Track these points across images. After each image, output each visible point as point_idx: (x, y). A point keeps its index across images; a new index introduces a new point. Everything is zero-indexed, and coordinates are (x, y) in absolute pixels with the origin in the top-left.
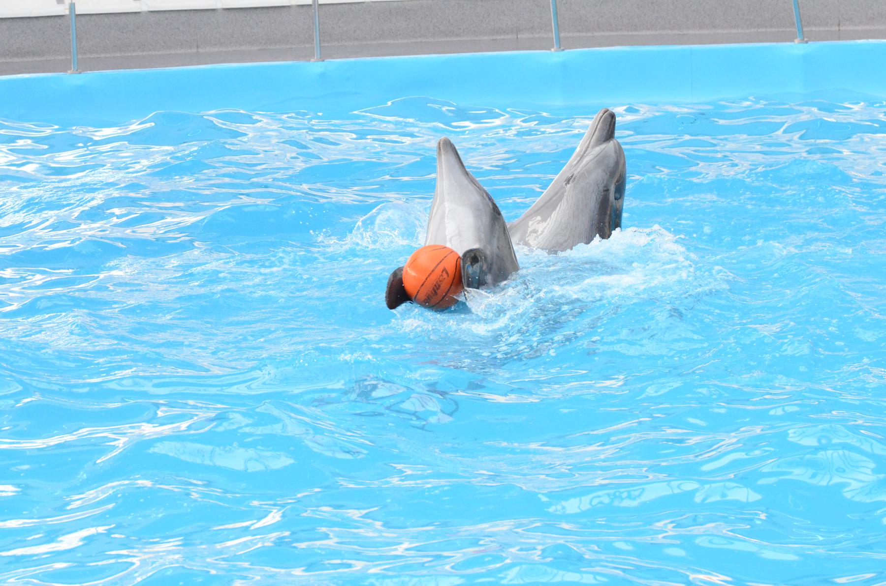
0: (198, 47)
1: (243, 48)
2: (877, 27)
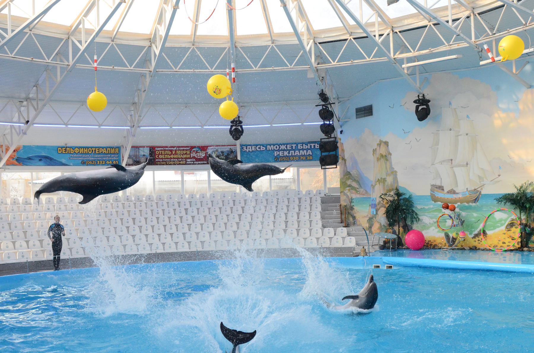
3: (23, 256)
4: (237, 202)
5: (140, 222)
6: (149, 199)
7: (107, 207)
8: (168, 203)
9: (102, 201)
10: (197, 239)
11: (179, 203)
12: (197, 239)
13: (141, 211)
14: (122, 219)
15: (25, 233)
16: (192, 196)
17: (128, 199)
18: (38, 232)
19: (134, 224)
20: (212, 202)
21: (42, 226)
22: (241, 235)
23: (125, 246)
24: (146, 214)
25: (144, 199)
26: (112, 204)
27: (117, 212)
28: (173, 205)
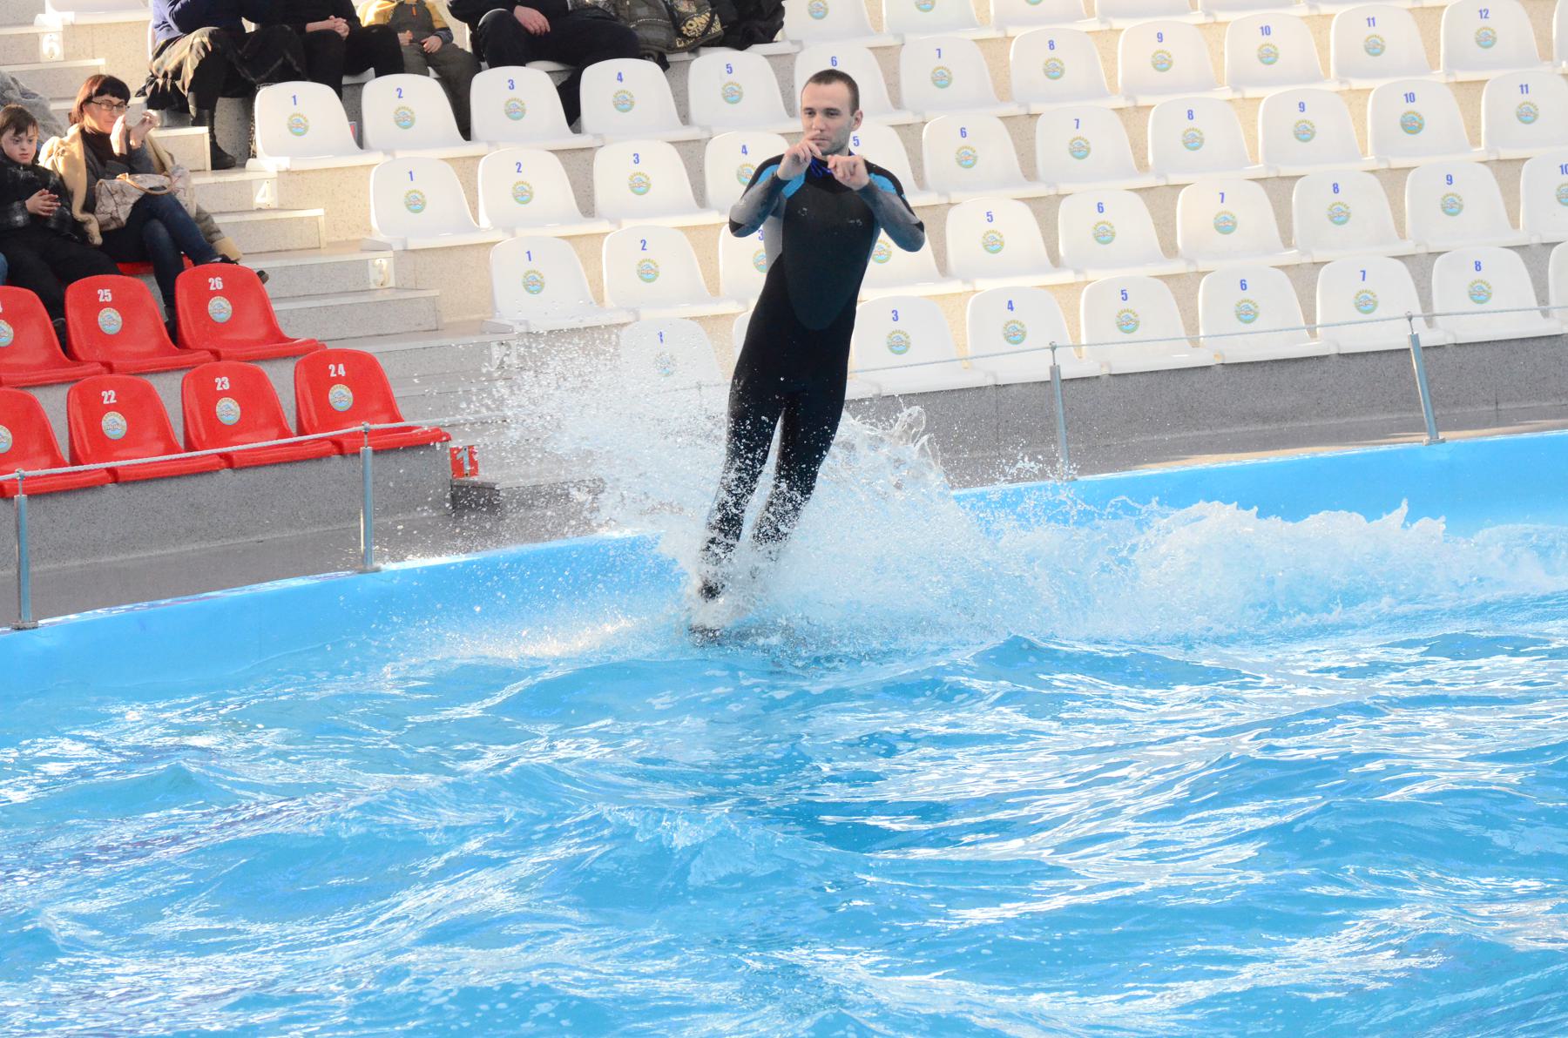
3: (1015, 335)
15: (1022, 126)
18: (1133, 116)
21: (1162, 63)
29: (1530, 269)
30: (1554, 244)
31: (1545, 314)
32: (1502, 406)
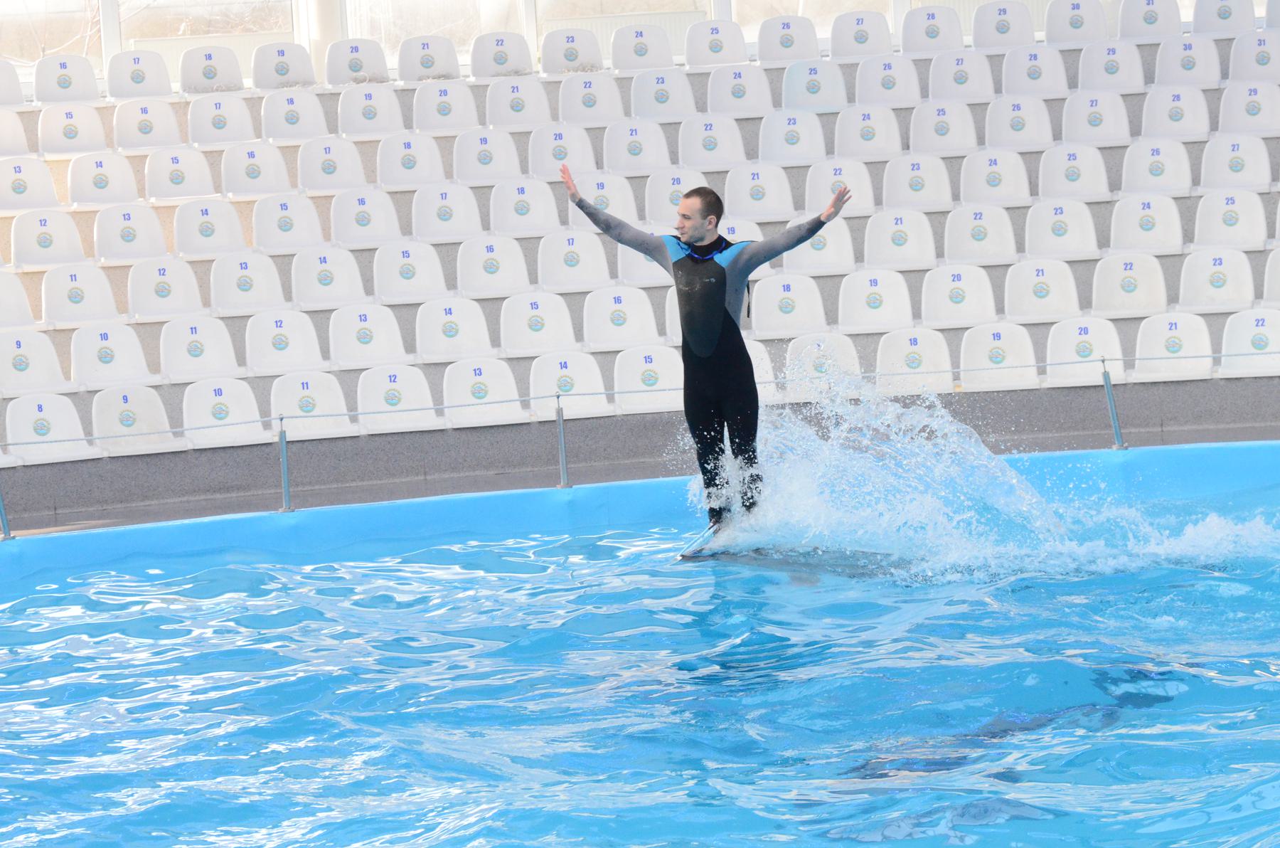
0: (425, 474)
1: (477, 473)
2: (1206, 426)
4: (1090, 65)
5: (445, 215)
6: (500, 59)
7: (219, 123)
8: (623, 83)
9: (189, 87)
10: (832, 317)
11: (699, 81)
12: (832, 317)
13: (446, 143)
14: (323, 203)
16: (785, 33)
17: (355, 66)
19: (406, 229)
20: (922, 66)
22: (1129, 287)
23: (348, 378)
24: (485, 159)
25: (465, 59)
26: (253, 103)
27: (289, 152)
28: (662, 98)
29: (79, 411)
30: (97, 392)
31: (90, 443)
32: (59, 511)
